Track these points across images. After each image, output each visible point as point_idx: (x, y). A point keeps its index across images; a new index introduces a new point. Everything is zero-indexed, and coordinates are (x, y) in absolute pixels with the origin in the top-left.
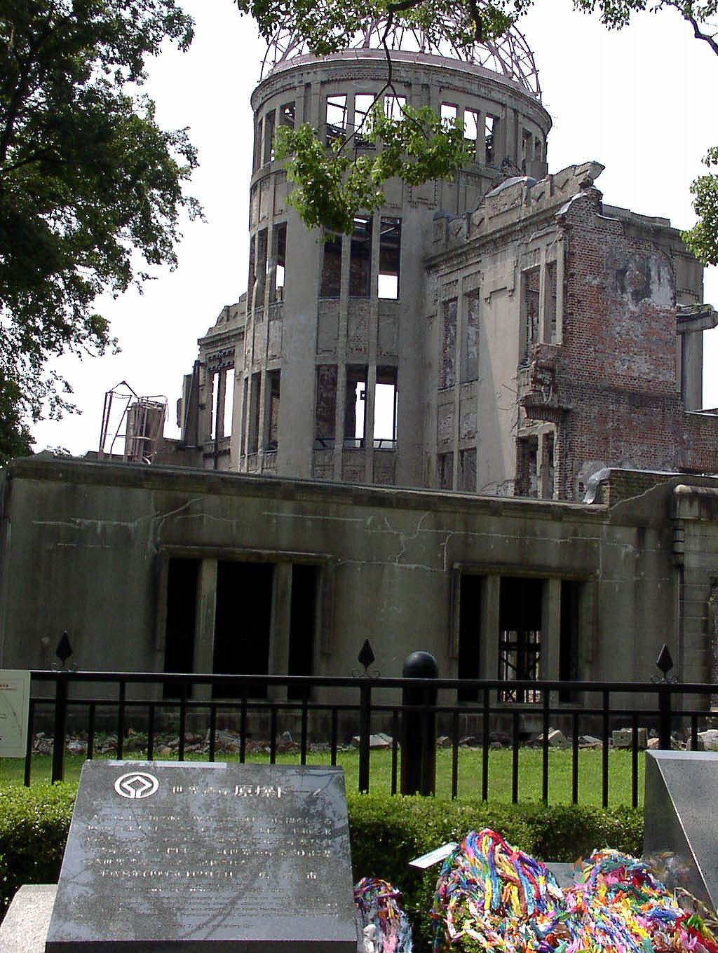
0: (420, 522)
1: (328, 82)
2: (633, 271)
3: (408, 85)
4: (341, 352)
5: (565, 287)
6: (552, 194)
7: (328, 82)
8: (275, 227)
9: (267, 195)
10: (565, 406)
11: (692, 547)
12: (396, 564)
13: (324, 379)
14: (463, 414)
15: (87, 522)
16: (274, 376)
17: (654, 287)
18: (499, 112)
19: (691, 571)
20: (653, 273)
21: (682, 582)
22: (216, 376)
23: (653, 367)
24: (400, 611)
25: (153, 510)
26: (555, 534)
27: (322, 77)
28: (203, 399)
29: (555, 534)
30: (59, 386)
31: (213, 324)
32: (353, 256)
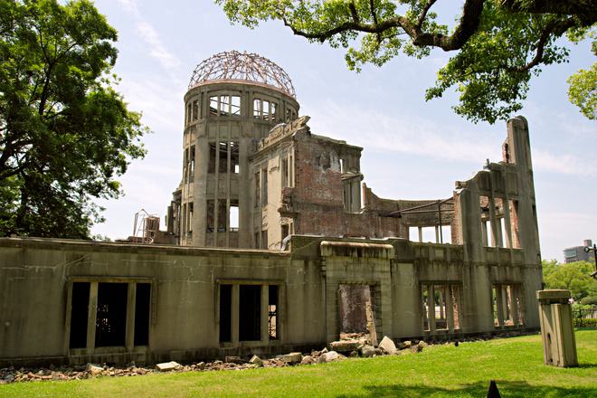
2: (323, 158)
4: (216, 195)
5: (295, 165)
8: (191, 147)
9: (189, 136)
12: (188, 281)
13: (210, 204)
15: (31, 267)
16: (191, 205)
17: (332, 164)
20: (332, 159)
26: (265, 265)
27: (208, 90)
28: (175, 215)
29: (266, 264)
30: (97, 210)
32: (220, 157)
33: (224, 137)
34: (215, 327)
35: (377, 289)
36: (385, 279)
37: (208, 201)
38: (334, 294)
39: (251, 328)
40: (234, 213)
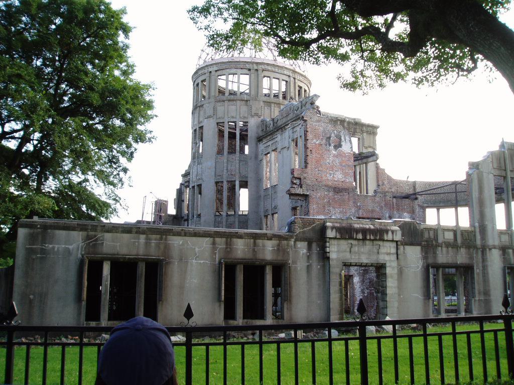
0: (206, 242)
1: (218, 70)
3: (250, 70)
4: (225, 177)
6: (302, 108)
7: (218, 70)
10: (305, 193)
11: (333, 249)
14: (273, 199)
15: (51, 246)
16: (200, 186)
17: (343, 144)
18: (286, 78)
19: (333, 260)
20: (342, 138)
21: (329, 265)
23: (344, 176)
24: (196, 281)
25: (81, 239)
31: (187, 168)
32: (229, 137)
33: (233, 117)
34: (220, 306)
35: (382, 271)
36: (391, 261)
37: (217, 183)
38: (338, 276)
39: (254, 309)
40: (244, 196)
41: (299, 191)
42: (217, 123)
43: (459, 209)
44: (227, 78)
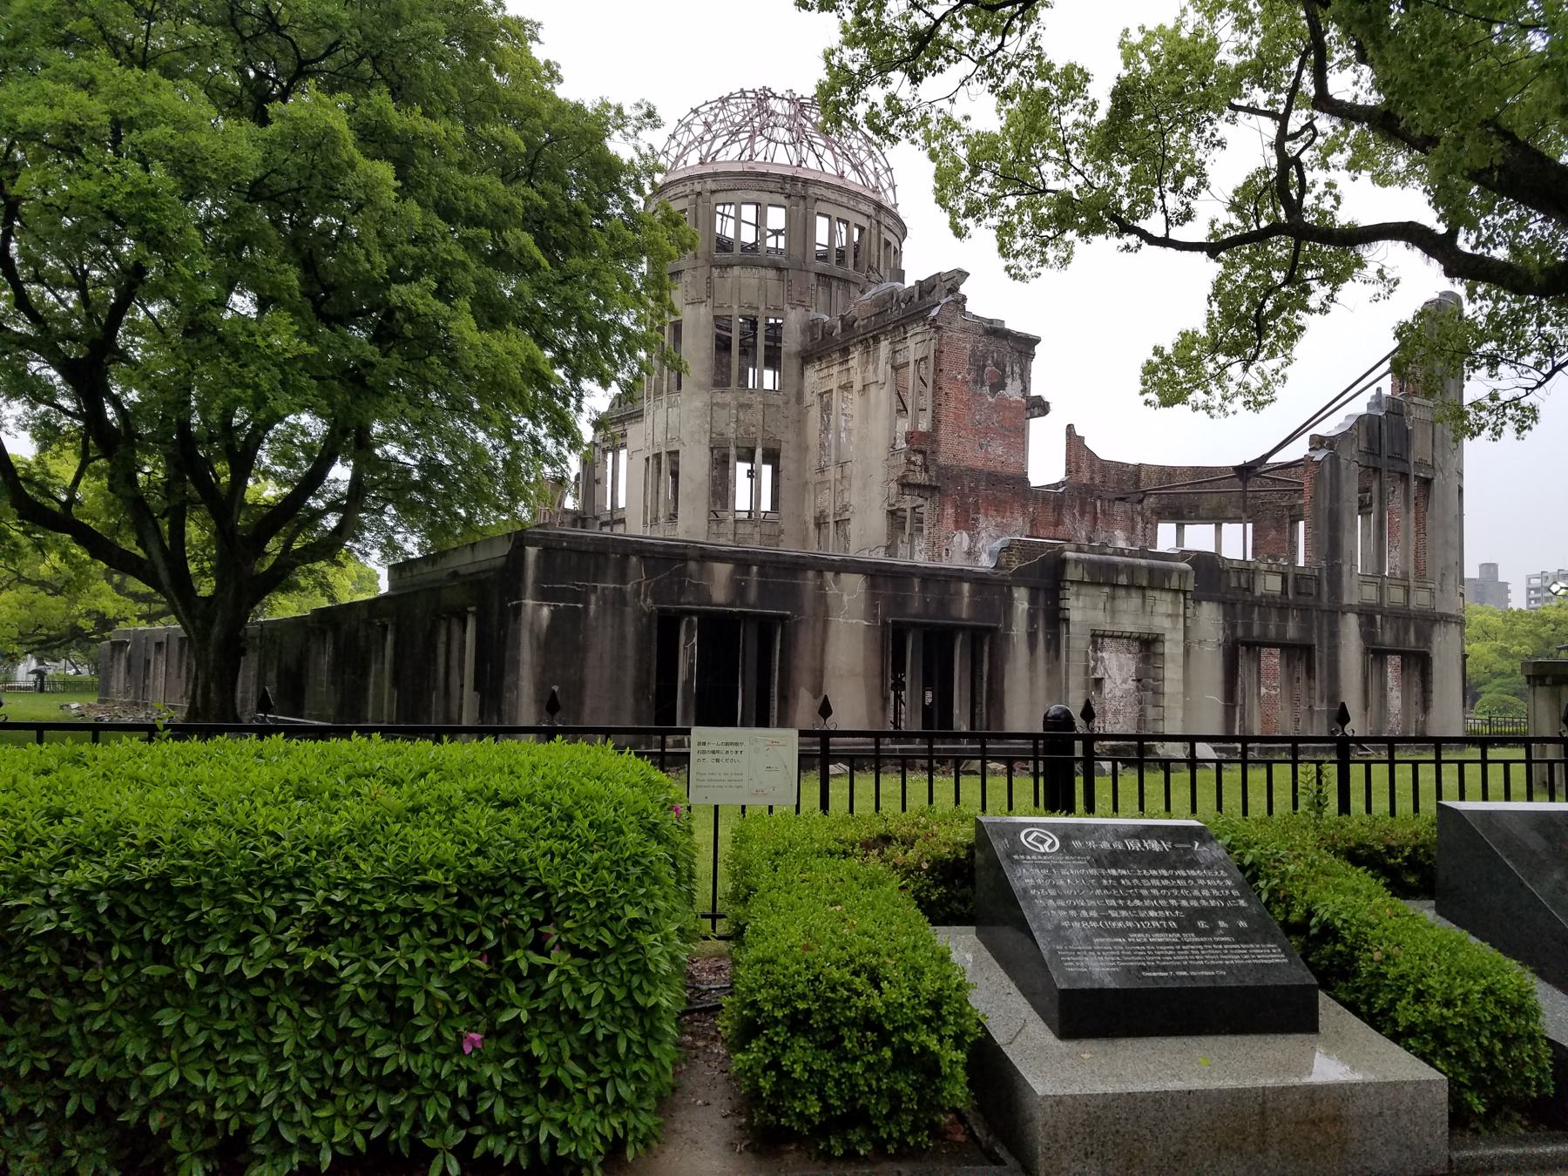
6: (921, 297)
17: (1009, 381)
18: (865, 223)
22: (610, 455)
27: (710, 185)
33: (750, 307)
41: (921, 478)
42: (716, 318)
43: (1225, 526)
44: (738, 212)
